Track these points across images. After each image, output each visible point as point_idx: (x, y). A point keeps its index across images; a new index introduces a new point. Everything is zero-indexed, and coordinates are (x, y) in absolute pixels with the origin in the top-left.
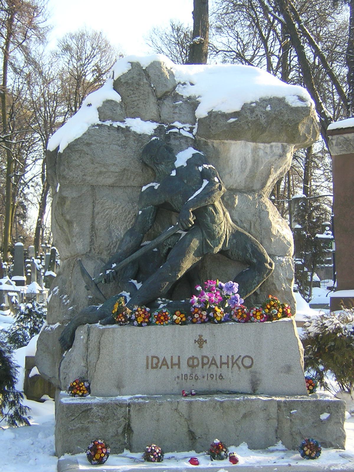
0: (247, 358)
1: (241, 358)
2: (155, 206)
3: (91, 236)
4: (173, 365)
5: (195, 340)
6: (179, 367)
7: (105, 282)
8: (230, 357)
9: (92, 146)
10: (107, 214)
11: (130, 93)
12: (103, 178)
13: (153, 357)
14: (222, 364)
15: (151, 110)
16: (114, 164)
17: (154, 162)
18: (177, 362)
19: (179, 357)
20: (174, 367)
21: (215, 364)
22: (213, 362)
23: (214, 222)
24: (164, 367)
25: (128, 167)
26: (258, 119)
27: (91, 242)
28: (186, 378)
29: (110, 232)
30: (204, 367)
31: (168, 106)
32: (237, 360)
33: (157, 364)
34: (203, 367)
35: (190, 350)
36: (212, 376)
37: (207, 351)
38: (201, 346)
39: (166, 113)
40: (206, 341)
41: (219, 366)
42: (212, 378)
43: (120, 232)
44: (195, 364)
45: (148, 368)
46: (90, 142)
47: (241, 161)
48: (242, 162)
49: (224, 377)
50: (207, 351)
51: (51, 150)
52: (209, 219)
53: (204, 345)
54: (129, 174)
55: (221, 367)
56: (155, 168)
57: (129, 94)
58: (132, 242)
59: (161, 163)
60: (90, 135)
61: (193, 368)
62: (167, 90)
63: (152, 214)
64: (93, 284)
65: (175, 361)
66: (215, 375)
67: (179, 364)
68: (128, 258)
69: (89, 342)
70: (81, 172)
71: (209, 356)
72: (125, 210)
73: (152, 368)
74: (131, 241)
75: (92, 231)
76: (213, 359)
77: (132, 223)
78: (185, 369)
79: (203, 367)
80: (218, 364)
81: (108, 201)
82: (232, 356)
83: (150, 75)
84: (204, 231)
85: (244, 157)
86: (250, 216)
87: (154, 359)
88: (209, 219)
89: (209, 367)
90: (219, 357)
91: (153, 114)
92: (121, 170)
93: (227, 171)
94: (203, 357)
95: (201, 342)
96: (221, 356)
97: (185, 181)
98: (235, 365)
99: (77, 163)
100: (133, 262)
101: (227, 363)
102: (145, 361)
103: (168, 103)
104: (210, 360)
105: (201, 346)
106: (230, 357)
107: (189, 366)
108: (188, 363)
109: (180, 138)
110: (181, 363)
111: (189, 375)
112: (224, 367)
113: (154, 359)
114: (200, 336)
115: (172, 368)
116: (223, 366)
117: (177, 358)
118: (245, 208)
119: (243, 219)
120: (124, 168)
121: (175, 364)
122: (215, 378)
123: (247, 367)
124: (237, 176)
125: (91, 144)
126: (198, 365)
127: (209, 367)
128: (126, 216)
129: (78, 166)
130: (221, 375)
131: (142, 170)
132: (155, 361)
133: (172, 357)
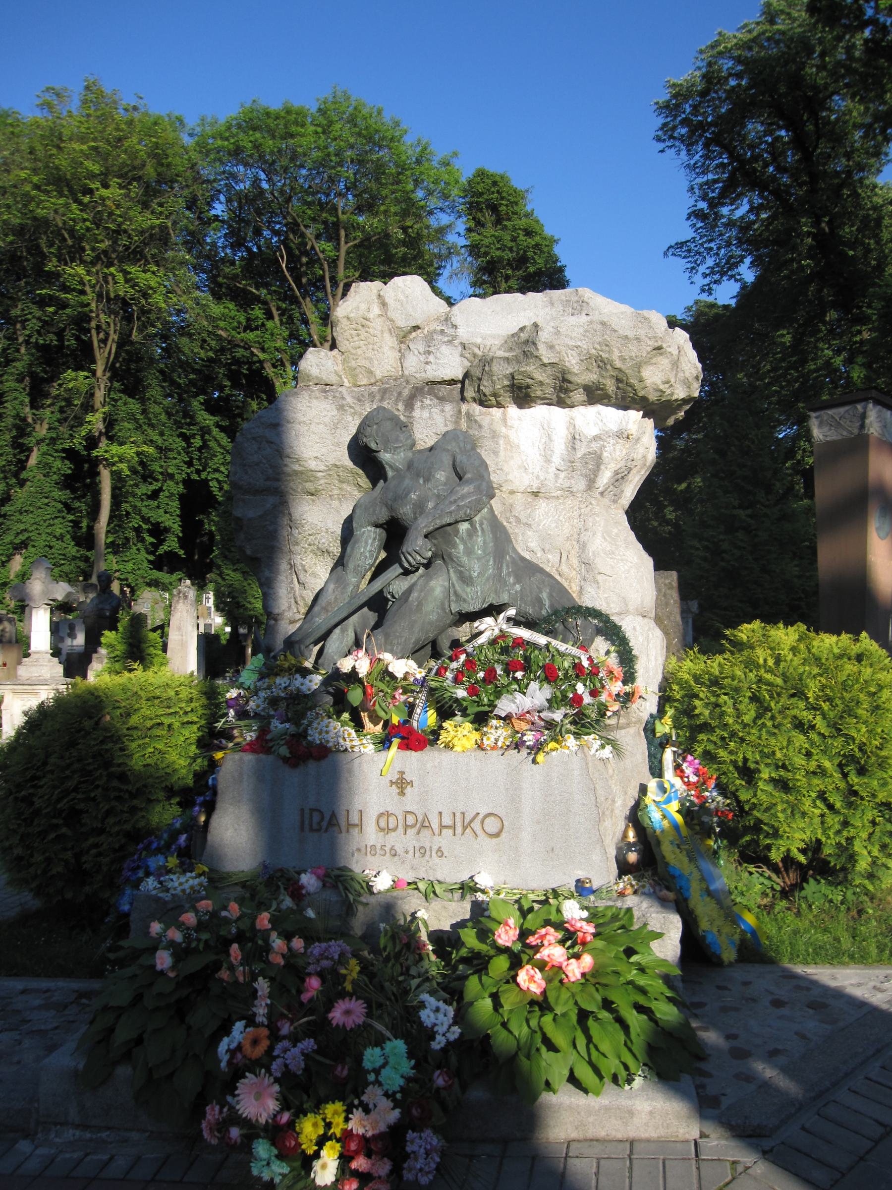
0: (492, 818)
5: (392, 783)
13: (312, 810)
14: (442, 827)
23: (469, 552)
30: (409, 831)
31: (416, 352)
33: (319, 823)
37: (411, 800)
41: (437, 831)
42: (423, 854)
44: (391, 826)
52: (461, 547)
53: (408, 790)
63: (370, 541)
66: (428, 849)
67: (360, 826)
73: (312, 830)
80: (435, 826)
82: (463, 814)
83: (387, 300)
84: (451, 571)
88: (461, 547)
89: (418, 833)
90: (436, 816)
91: (389, 368)
95: (401, 784)
96: (440, 813)
98: (468, 830)
103: (418, 346)
104: (420, 819)
105: (402, 793)
107: (382, 830)
111: (378, 847)
112: (448, 832)
116: (444, 831)
118: (553, 525)
119: (547, 547)
122: (428, 853)
123: (492, 836)
124: (538, 469)
126: (395, 829)
127: (418, 833)
129: (257, 464)
130: (439, 850)
132: (316, 817)
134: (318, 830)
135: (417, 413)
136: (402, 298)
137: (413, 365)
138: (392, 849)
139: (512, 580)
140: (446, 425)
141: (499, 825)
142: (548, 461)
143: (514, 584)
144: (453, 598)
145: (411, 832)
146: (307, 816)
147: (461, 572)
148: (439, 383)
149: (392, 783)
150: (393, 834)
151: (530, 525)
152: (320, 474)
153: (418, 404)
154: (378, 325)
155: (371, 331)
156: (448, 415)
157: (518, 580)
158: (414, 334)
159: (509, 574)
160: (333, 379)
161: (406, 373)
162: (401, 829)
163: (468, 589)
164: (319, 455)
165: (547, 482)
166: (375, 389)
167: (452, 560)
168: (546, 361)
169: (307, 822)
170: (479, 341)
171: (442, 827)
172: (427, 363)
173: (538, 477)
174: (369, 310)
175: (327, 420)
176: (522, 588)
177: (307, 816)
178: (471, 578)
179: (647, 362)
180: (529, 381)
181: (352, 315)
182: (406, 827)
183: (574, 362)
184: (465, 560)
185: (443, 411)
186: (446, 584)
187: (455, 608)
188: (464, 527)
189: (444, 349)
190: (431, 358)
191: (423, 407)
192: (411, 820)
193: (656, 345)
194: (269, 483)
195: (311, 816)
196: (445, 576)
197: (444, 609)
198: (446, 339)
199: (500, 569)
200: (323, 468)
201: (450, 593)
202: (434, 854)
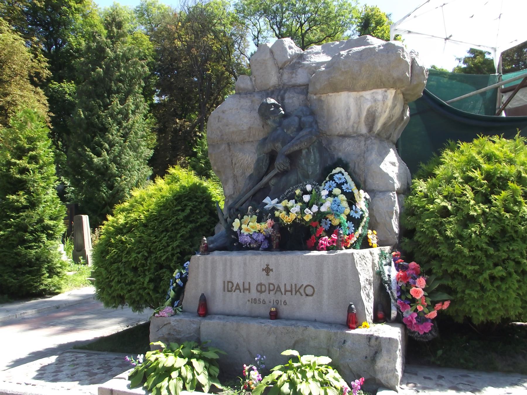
0: (310, 287)
1: (304, 286)
2: (267, 154)
4: (244, 289)
5: (263, 270)
6: (249, 292)
8: (293, 285)
9: (227, 112)
10: (241, 164)
13: (228, 282)
14: (286, 291)
19: (249, 283)
21: (280, 291)
22: (279, 289)
24: (237, 291)
27: (234, 187)
30: (271, 292)
38: (268, 275)
40: (272, 270)
41: (283, 293)
44: (263, 290)
45: (224, 291)
47: (346, 110)
49: (288, 303)
53: (271, 273)
55: (285, 294)
65: (247, 286)
67: (249, 289)
70: (220, 132)
71: (274, 284)
73: (228, 291)
76: (279, 287)
78: (254, 294)
80: (283, 290)
87: (229, 283)
88: (303, 161)
93: (334, 120)
94: (270, 284)
95: (268, 270)
96: (285, 285)
97: (285, 131)
98: (298, 293)
101: (291, 291)
102: (222, 285)
104: (276, 287)
105: (268, 275)
107: (258, 291)
111: (257, 299)
113: (229, 283)
114: (268, 265)
115: (244, 292)
116: (287, 293)
121: (247, 289)
122: (280, 303)
124: (344, 123)
126: (265, 291)
130: (285, 302)
131: (263, 127)
133: (244, 283)
134: (231, 291)
138: (263, 300)
141: (312, 290)
142: (348, 119)
145: (272, 293)
146: (226, 284)
149: (263, 270)
150: (264, 293)
154: (270, 63)
162: (267, 291)
172: (292, 78)
177: (226, 284)
185: (298, 99)
186: (296, 178)
188: (304, 152)
190: (294, 75)
191: (289, 98)
202: (282, 303)
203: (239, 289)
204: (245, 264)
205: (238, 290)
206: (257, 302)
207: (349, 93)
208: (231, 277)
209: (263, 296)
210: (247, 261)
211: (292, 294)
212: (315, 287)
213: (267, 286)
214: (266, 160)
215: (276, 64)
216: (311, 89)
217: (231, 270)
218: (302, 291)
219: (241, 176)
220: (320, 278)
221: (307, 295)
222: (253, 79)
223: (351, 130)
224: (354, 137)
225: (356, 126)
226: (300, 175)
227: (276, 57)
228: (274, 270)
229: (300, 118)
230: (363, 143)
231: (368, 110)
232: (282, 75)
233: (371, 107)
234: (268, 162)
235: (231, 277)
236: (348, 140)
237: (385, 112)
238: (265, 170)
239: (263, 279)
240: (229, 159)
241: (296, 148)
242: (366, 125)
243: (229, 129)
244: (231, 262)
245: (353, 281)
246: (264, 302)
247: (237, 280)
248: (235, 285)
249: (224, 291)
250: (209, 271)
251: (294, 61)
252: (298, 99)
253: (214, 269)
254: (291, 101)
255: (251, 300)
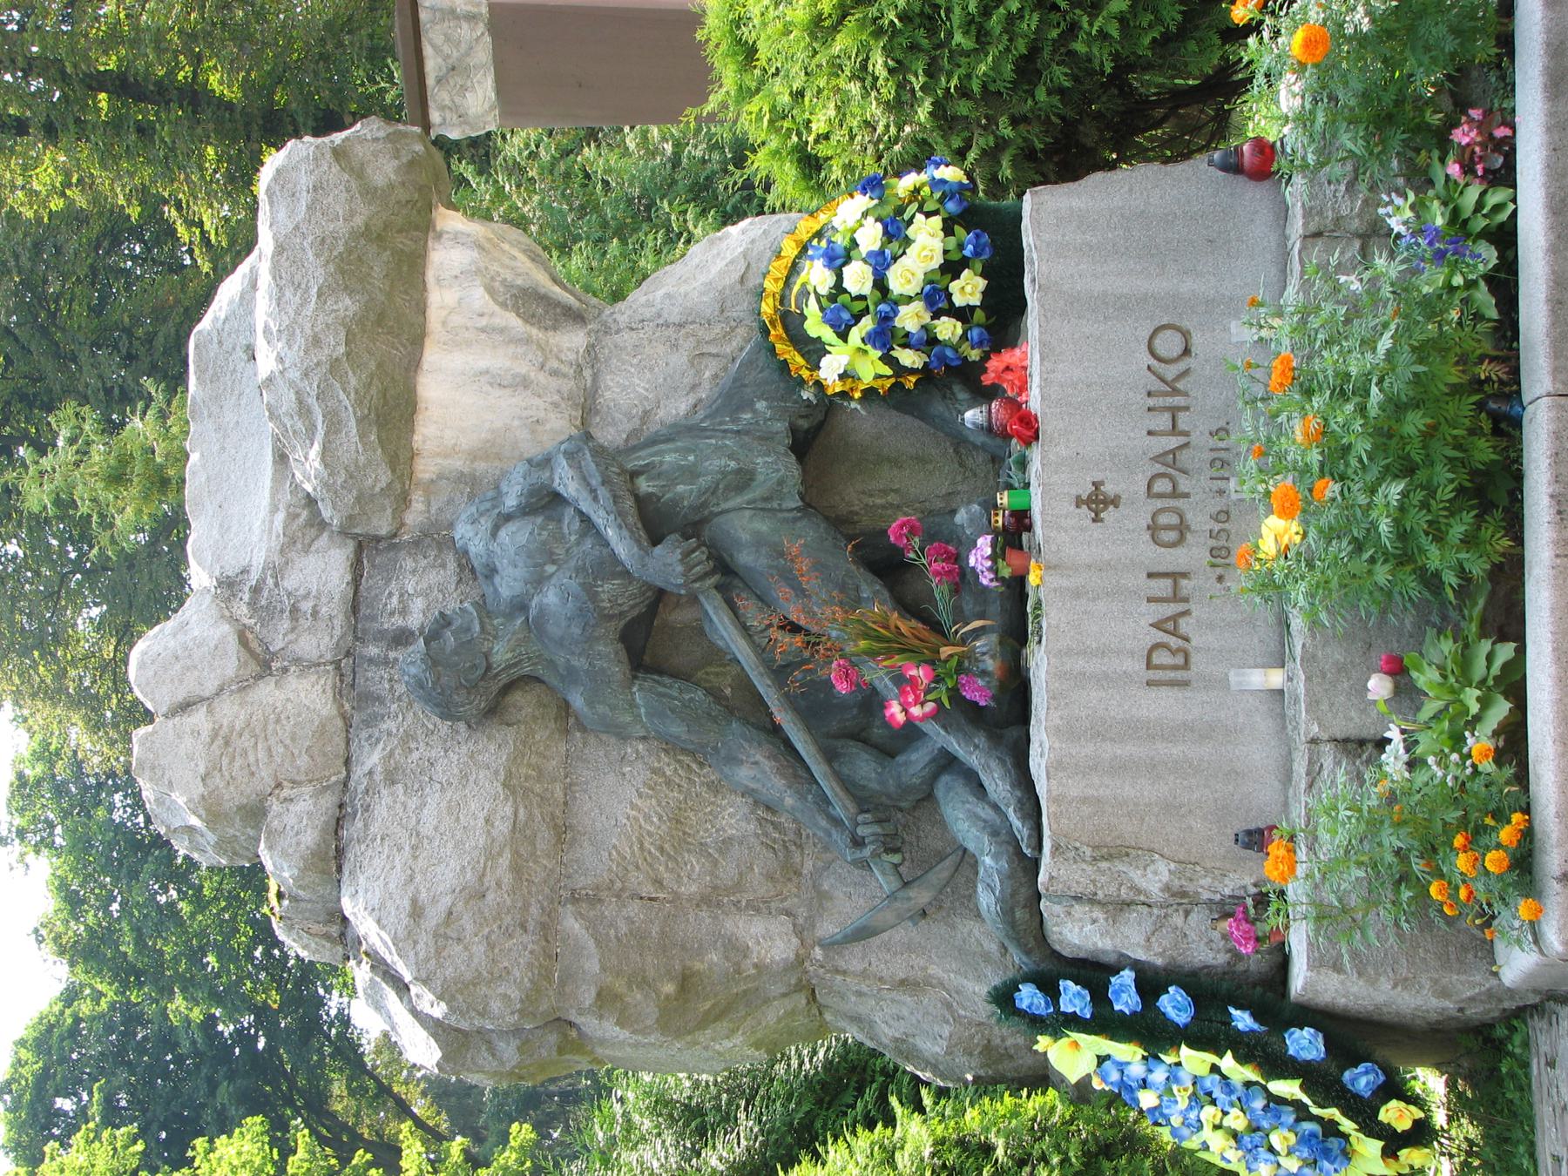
0: (1157, 342)
3: (739, 909)
4: (1176, 597)
6: (1184, 575)
7: (896, 850)
8: (1151, 402)
9: (423, 895)
10: (661, 849)
11: (242, 769)
12: (536, 862)
13: (1149, 666)
14: (1174, 430)
15: (302, 695)
16: (487, 821)
17: (483, 677)
18: (1168, 582)
20: (1184, 593)
21: (1173, 452)
23: (691, 473)
24: (1185, 625)
25: (496, 772)
26: (344, 325)
27: (758, 910)
28: (1223, 553)
29: (724, 841)
31: (291, 637)
32: (1163, 380)
33: (1174, 653)
34: (1187, 495)
35: (1125, 538)
36: (1218, 464)
38: (1115, 502)
39: (314, 642)
40: (1096, 485)
42: (1224, 463)
43: (724, 809)
44: (1175, 520)
46: (407, 903)
47: (487, 388)
48: (491, 384)
49: (1222, 423)
50: (1128, 484)
51: (438, 1054)
52: (680, 488)
53: (1109, 489)
54: (523, 770)
56: (504, 679)
57: (246, 771)
58: (758, 757)
59: (487, 656)
60: (382, 906)
61: (1188, 528)
62: (233, 640)
63: (661, 689)
64: (900, 894)
65: (1163, 587)
67: (1176, 576)
68: (813, 768)
69: (1100, 895)
71: (1149, 474)
72: (651, 788)
73: (1186, 665)
74: (756, 763)
75: (719, 905)
76: (1156, 459)
77: (694, 766)
78: (1192, 555)
79: (1187, 495)
80: (1174, 442)
81: (615, 847)
85: (475, 375)
86: (680, 359)
87: (1156, 660)
88: (680, 488)
92: (506, 799)
94: (1150, 492)
95: (1097, 502)
96: (1150, 433)
98: (1179, 385)
99: (479, 949)
100: (830, 756)
101: (1174, 411)
102: (1164, 692)
104: (1163, 469)
105: (1115, 502)
106: (1151, 402)
107: (1181, 540)
108: (1173, 545)
109: (401, 595)
110: (1171, 569)
111: (1213, 543)
112: (1183, 420)
114: (1079, 502)
115: (1186, 600)
116: (1182, 426)
117: (1153, 583)
119: (688, 380)
120: (500, 789)
122: (1223, 455)
124: (537, 401)
125: (414, 901)
128: (668, 783)
129: (491, 946)
132: (1161, 658)
133: (1149, 600)
135: (415, 620)
136: (178, 667)
137: (316, 643)
139: (749, 416)
140: (443, 566)
141: (1169, 332)
142: (524, 383)
143: (755, 411)
144: (775, 505)
145: (1184, 484)
147: (727, 488)
148: (356, 593)
150: (1189, 516)
151: (646, 412)
152: (522, 811)
153: (398, 621)
154: (230, 711)
155: (238, 725)
156: (424, 563)
157: (749, 405)
158: (254, 645)
159: (735, 421)
160: (329, 801)
161: (329, 657)
162: (1178, 503)
163: (760, 478)
164: (481, 815)
165: (565, 389)
166: (356, 720)
167: (704, 505)
168: (342, 349)
169: (1171, 675)
170: (281, 516)
171: (1174, 430)
172: (315, 613)
173: (556, 405)
174: (196, 733)
175: (413, 803)
176: (761, 397)
178: (739, 471)
179: (359, 173)
180: (374, 391)
181: (202, 770)
182: (1175, 494)
183: (348, 301)
184: (703, 482)
185: (414, 572)
186: (747, 513)
187: (796, 502)
188: (644, 485)
189: (289, 583)
190: (306, 606)
191: (404, 611)
192: (1162, 486)
193: (328, 156)
194: (531, 926)
195: (1158, 667)
196: (731, 515)
197: (795, 520)
198: (270, 581)
199: (725, 431)
200: (509, 810)
201: (764, 507)
202: (1222, 445)
203: (1174, 618)
204: (1077, 594)
205: (1182, 622)
206: (1222, 543)
207: (425, 365)
208: (1132, 654)
209: (1200, 520)
210: (1065, 583)
211: (1187, 408)
212: (1157, 324)
213: (1159, 504)
214: (658, 682)
215: (243, 686)
216: (383, 526)
217: (1102, 652)
218: (1170, 372)
219: (715, 863)
220: (1124, 306)
221: (1187, 352)
222: (286, 793)
223: (568, 385)
224: (595, 377)
225: (555, 364)
226: (737, 501)
227: (210, 688)
228: (1098, 477)
229: (508, 518)
230: (627, 338)
231: (504, 305)
232: (297, 661)
233: (490, 291)
234: (667, 680)
235: (1132, 654)
236: (608, 394)
237: (515, 258)
238: (700, 694)
239: (1132, 518)
240: (634, 909)
241: (629, 503)
242: (555, 329)
243: (499, 885)
244: (1069, 652)
245: (1131, 190)
246: (1223, 515)
247: (1136, 627)
248: (1161, 637)
249: (1184, 684)
250: (1109, 750)
251: (241, 610)
252: (414, 572)
253: (1099, 731)
254: (418, 604)
255: (1219, 571)
